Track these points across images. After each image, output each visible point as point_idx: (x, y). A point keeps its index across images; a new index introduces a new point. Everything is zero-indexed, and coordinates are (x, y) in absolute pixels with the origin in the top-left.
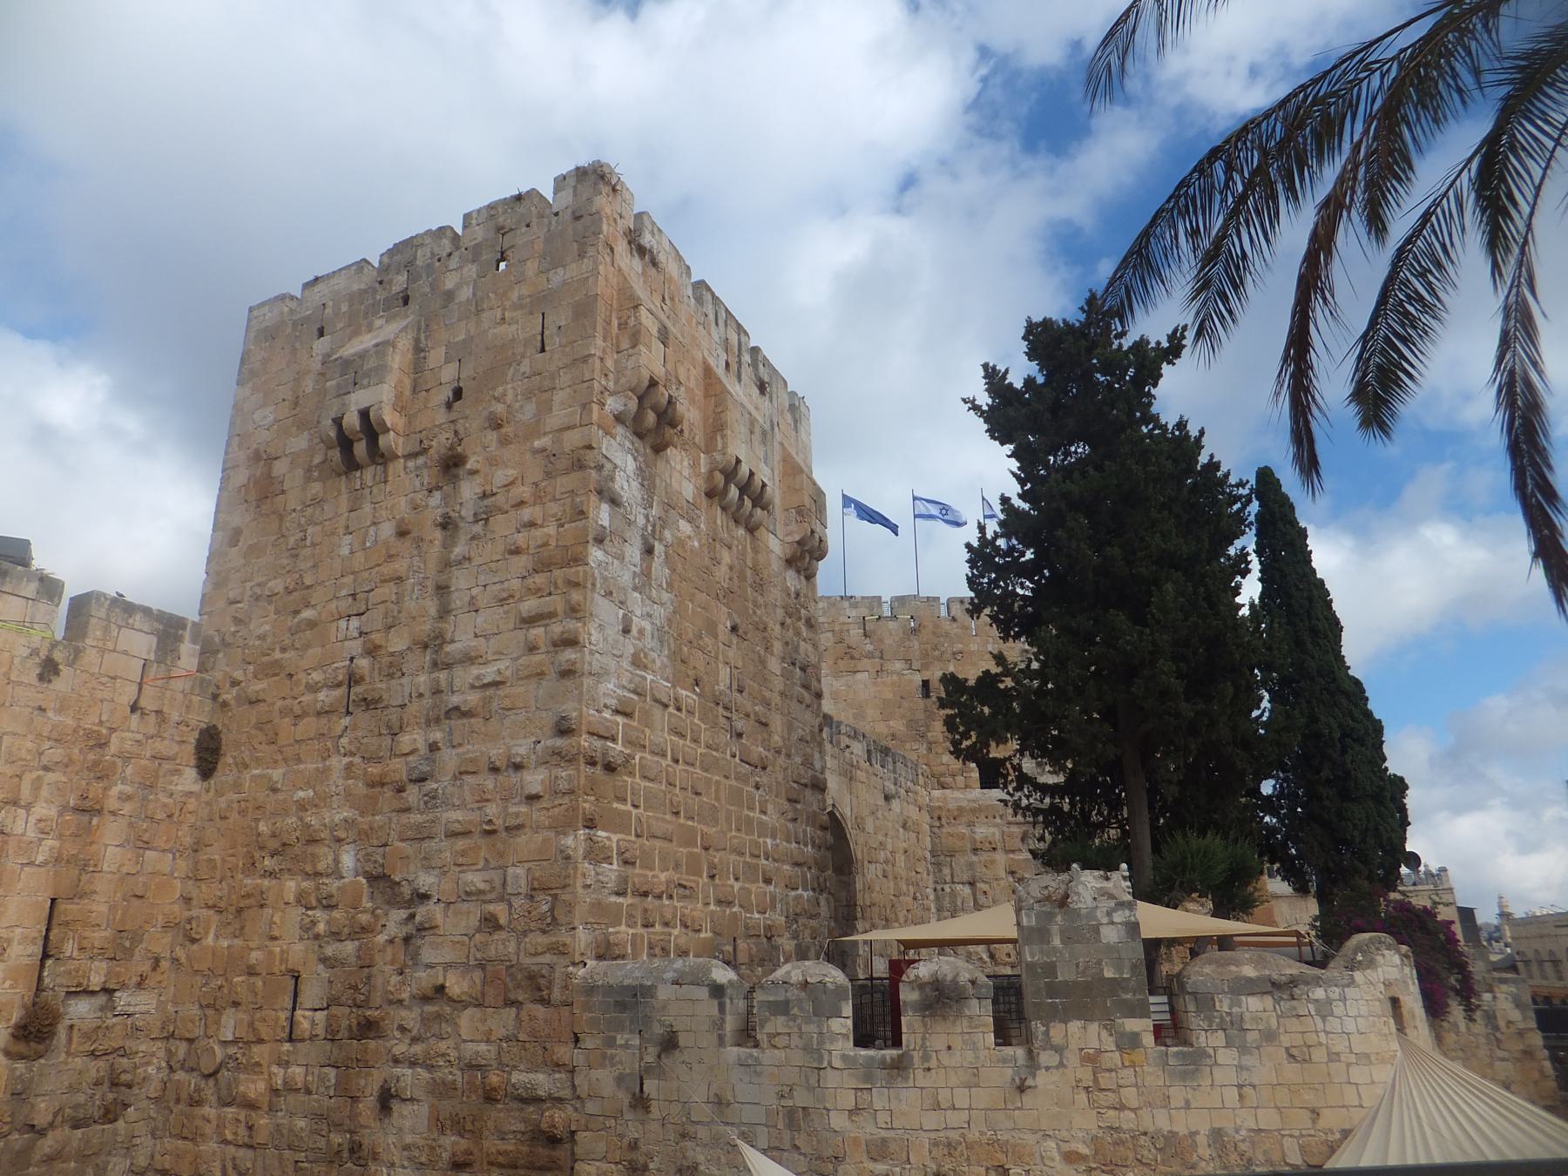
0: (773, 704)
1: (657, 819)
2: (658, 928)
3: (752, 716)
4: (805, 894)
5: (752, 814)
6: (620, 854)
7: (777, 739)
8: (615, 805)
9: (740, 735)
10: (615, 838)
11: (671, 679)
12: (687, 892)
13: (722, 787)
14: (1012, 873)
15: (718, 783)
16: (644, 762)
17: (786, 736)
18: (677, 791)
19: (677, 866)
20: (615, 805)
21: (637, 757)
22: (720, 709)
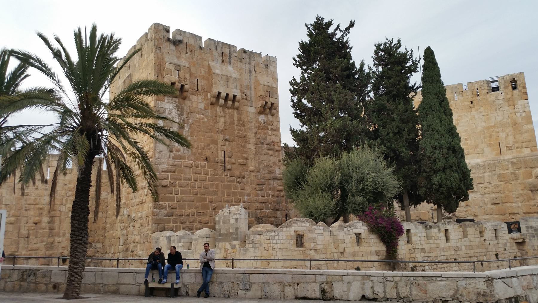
0: (249, 158)
1: (187, 197)
2: (187, 223)
3: (237, 163)
4: (267, 211)
5: (236, 191)
6: (169, 206)
7: (251, 168)
8: (167, 195)
9: (229, 170)
10: (167, 203)
11: (193, 159)
12: (202, 214)
13: (220, 186)
15: (217, 185)
16: (180, 183)
17: (257, 166)
18: (196, 188)
19: (197, 208)
20: (167, 195)
21: (177, 182)
22: (219, 164)
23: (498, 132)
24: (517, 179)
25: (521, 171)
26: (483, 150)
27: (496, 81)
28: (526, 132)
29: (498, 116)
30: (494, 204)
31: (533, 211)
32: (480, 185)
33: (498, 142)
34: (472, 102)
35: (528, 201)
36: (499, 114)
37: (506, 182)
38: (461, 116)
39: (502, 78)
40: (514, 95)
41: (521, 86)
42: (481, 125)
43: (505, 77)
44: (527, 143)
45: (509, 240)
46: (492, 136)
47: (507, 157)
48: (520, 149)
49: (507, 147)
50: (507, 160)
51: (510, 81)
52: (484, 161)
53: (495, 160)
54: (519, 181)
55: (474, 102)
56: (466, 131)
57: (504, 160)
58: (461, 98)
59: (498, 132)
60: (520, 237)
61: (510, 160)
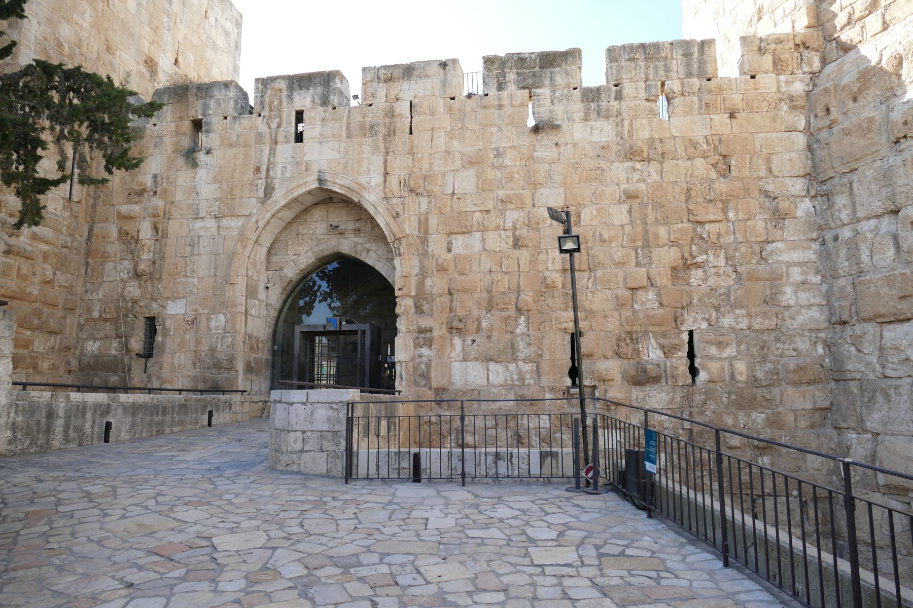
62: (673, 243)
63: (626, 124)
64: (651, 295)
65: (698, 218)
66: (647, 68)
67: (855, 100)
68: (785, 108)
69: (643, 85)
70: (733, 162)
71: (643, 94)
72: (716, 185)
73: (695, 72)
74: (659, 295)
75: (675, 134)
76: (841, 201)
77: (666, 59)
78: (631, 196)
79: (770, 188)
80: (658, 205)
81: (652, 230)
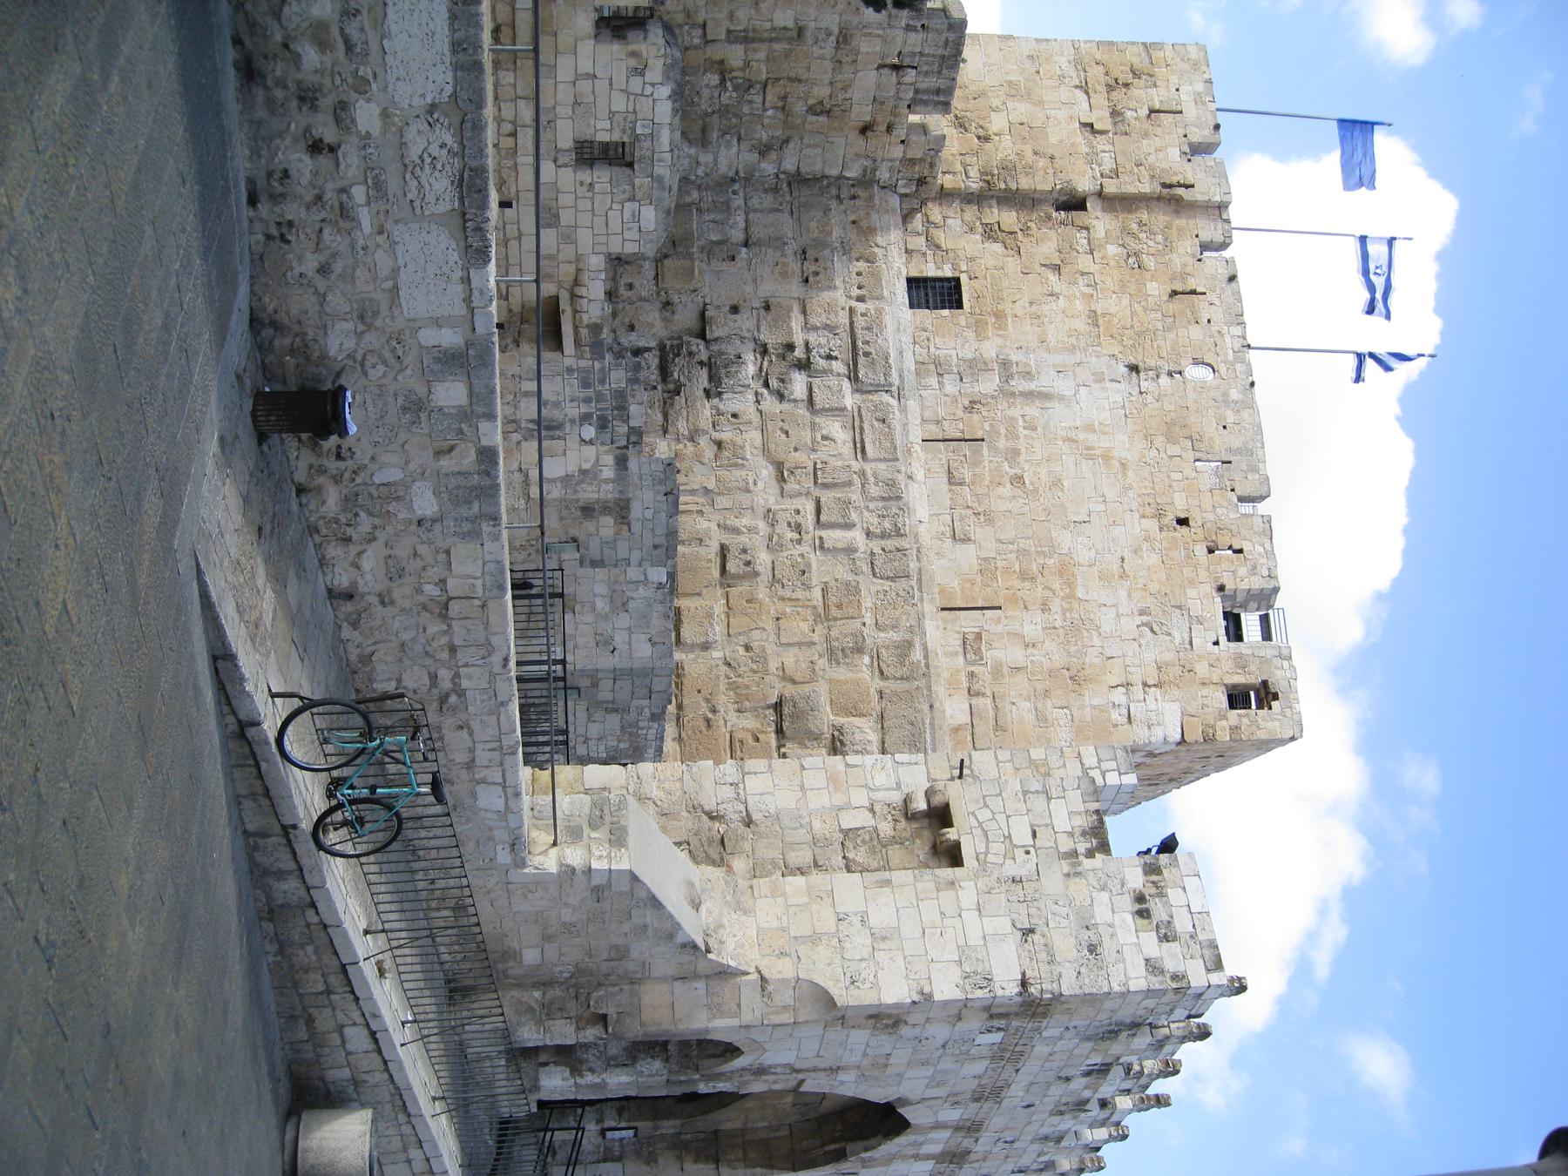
14: (767, 308)
23: (1045, 608)
24: (831, 654)
25: (866, 674)
26: (966, 540)
27: (1267, 636)
28: (1041, 718)
29: (1118, 616)
30: (724, 551)
31: (686, 702)
32: (810, 507)
33: (1001, 602)
34: (1183, 522)
35: (733, 687)
36: (1123, 619)
37: (824, 616)
38: (1125, 475)
39: (1285, 652)
40: (1205, 691)
41: (1245, 720)
42: (1080, 547)
43: (1286, 664)
44: (991, 714)
45: (568, 252)
46: (1027, 584)
47: (929, 625)
48: (965, 685)
49: (979, 636)
50: (918, 628)
51: (1265, 683)
52: (916, 535)
53: (920, 580)
54: (822, 663)
55: (1184, 529)
56: (1057, 483)
57: (920, 618)
58: (1207, 481)
59: (1045, 608)
60: (585, 318)
61: (917, 640)
62: (747, 64)
63: (880, 32)
64: (696, 41)
65: (769, 87)
66: (933, 56)
67: (854, 222)
68: (866, 163)
69: (918, 49)
70: (822, 119)
71: (906, 50)
72: (800, 104)
73: (919, 96)
74: (696, 47)
75: (859, 75)
76: (769, 200)
77: (940, 73)
78: (801, 31)
79: (791, 145)
80: (787, 55)
81: (764, 46)
